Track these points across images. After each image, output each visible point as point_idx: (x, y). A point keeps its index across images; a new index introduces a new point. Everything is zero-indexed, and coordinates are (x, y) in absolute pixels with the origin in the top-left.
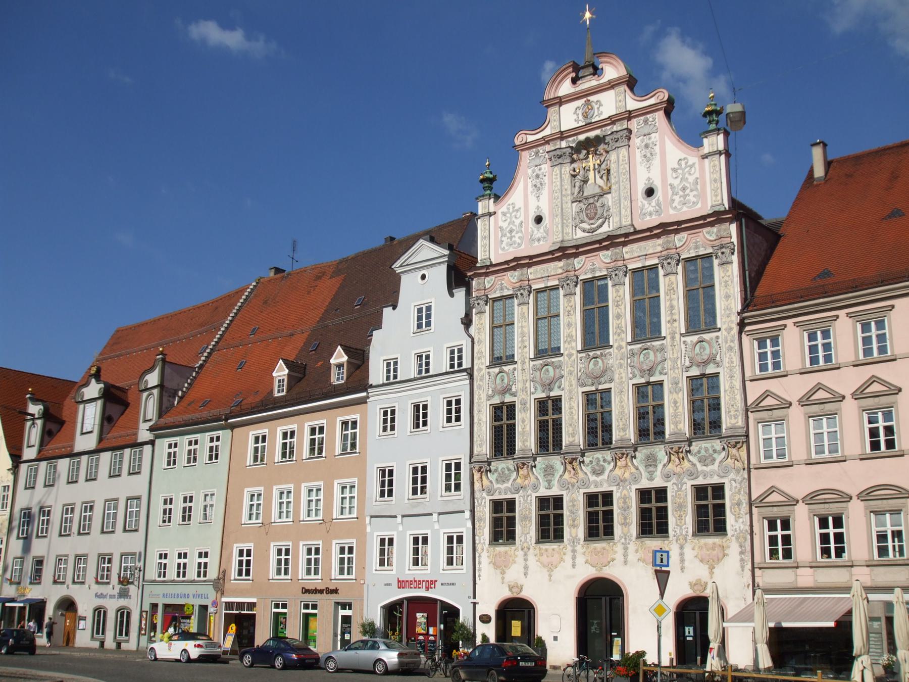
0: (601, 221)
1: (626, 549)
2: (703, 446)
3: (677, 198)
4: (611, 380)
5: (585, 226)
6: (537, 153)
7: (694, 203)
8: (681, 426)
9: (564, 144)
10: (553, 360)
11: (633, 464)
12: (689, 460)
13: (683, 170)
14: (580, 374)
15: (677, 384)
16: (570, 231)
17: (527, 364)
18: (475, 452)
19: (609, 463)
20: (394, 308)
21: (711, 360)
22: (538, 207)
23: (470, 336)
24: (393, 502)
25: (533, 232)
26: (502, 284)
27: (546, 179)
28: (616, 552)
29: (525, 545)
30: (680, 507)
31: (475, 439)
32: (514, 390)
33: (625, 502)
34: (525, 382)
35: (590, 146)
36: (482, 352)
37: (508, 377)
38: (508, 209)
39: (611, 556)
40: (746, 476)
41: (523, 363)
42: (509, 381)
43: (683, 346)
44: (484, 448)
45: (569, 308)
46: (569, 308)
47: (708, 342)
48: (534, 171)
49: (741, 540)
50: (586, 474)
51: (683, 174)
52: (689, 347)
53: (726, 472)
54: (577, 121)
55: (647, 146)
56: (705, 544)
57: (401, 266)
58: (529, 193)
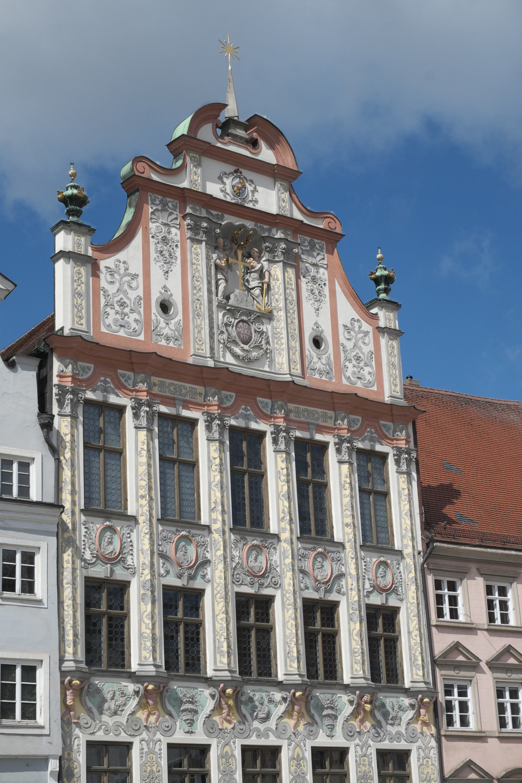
4: (276, 585)
25: (158, 322)
26: (105, 382)
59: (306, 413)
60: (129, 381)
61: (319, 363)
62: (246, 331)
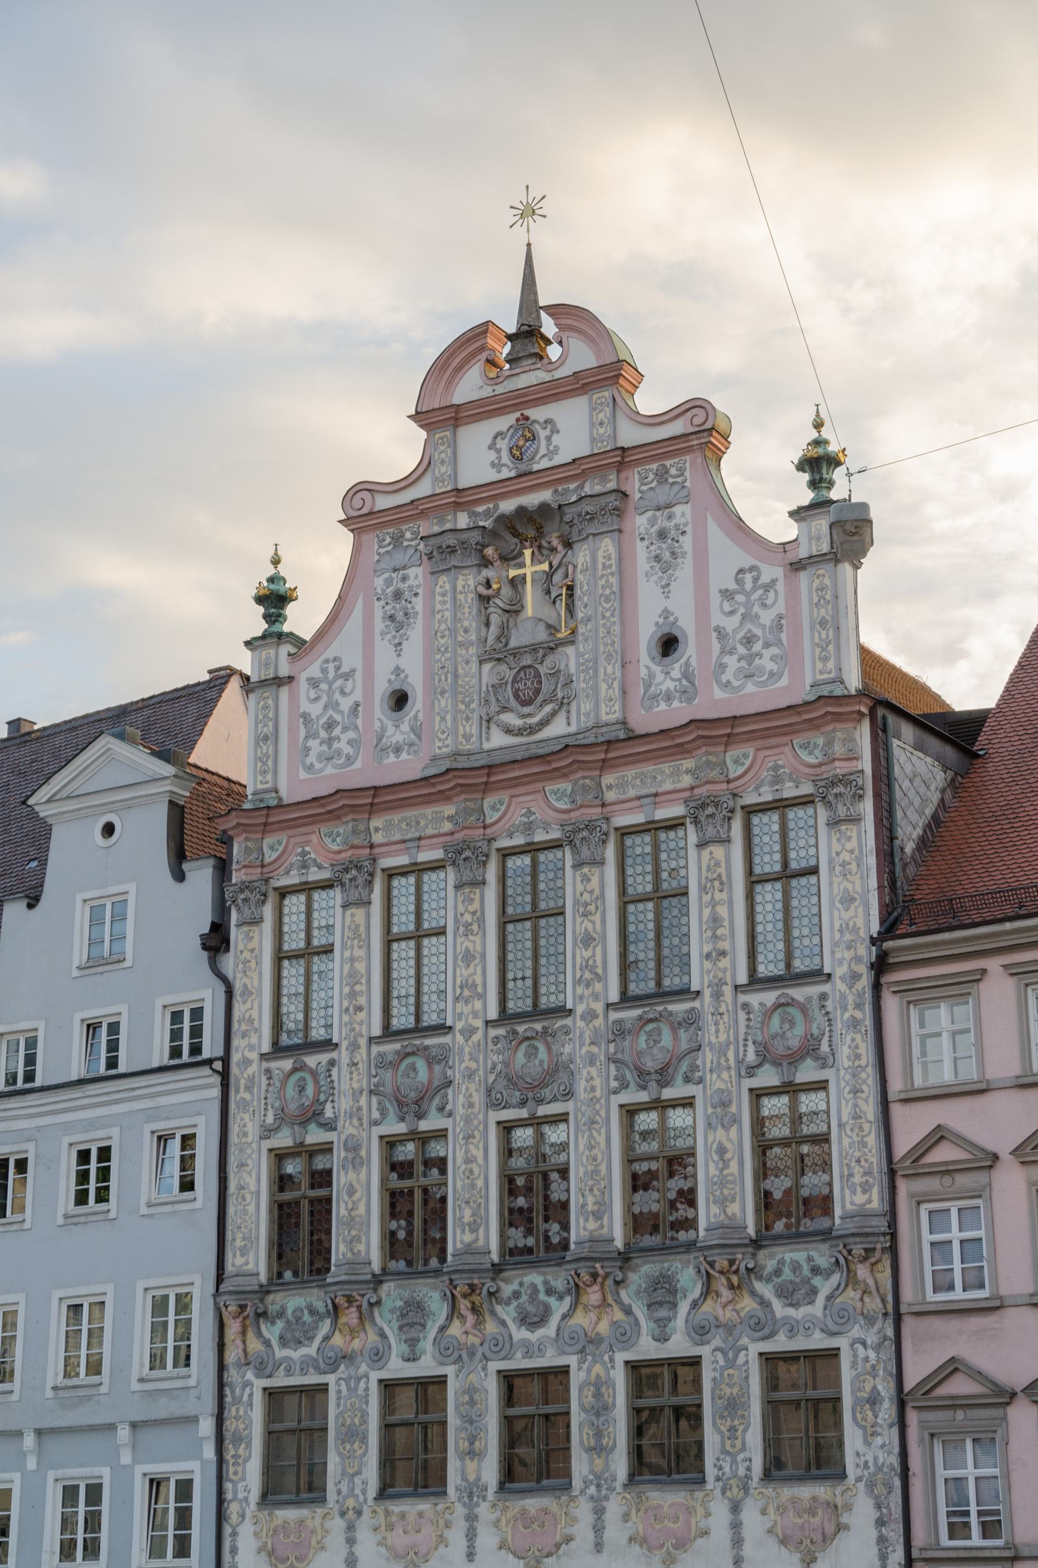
0: (548, 708)
1: (599, 1512)
2: (788, 1257)
3: (732, 662)
4: (568, 1094)
5: (512, 719)
6: (397, 540)
7: (772, 674)
8: (734, 1208)
9: (463, 520)
10: (428, 1042)
11: (619, 1302)
12: (753, 1293)
13: (748, 595)
14: (492, 1078)
15: (725, 1104)
16: (474, 732)
17: (363, 1050)
18: (229, 1268)
19: (561, 1298)
20: (30, 906)
21: (809, 1049)
22: (398, 671)
23: (224, 979)
24: (15, 1397)
25: (383, 729)
26: (304, 854)
27: (418, 604)
28: (575, 1520)
29: (350, 1503)
30: (733, 1407)
31: (229, 1236)
32: (329, 1113)
33: (598, 1395)
34: (356, 1094)
35: (527, 528)
36: (251, 1021)
37: (316, 1082)
38: (324, 671)
39: (561, 1530)
40: (890, 1332)
41: (354, 1047)
42: (318, 1092)
43: (742, 1016)
44: (252, 1258)
45: (468, 917)
46: (468, 917)
47: (804, 1009)
48: (388, 582)
49: (879, 1489)
50: (503, 1323)
51: (748, 605)
52: (756, 1018)
53: (842, 1320)
54: (496, 465)
55: (662, 535)
56: (794, 1501)
57: (49, 801)
58: (377, 637)
59: (638, 782)
60: (338, 840)
61: (668, 680)
62: (529, 683)
